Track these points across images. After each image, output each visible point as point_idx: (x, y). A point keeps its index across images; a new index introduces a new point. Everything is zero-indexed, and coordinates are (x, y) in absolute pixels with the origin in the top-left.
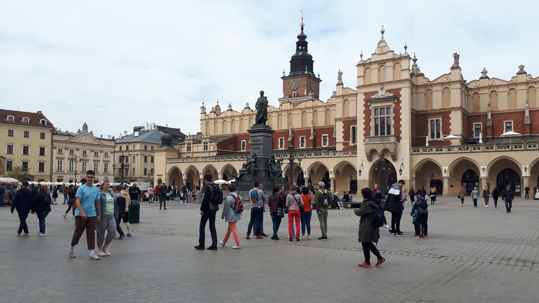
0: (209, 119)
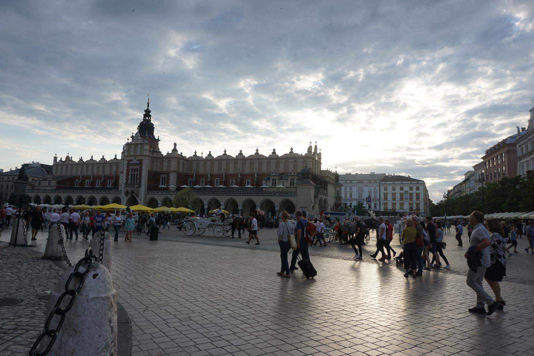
0: (59, 165)
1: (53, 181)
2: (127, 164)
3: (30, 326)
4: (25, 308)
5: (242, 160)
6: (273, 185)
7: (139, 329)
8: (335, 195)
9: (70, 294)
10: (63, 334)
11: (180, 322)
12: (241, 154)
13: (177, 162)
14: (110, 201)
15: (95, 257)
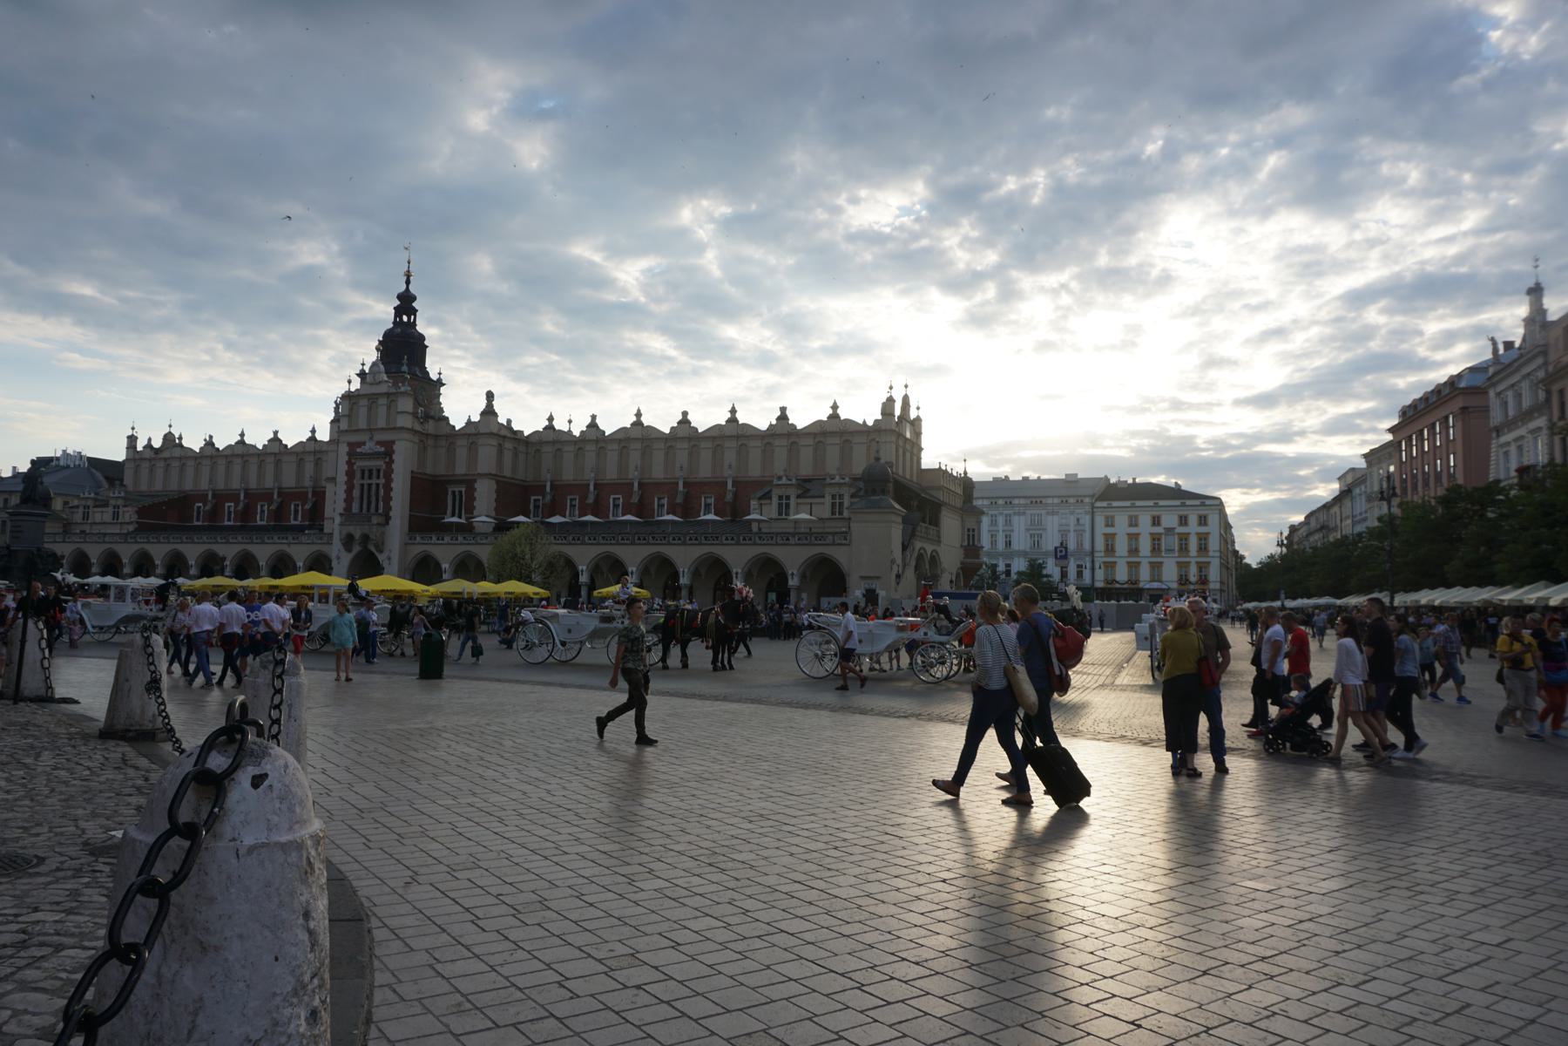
1: (125, 509)
2: (349, 454)
3: (65, 935)
4: (50, 883)
5: (689, 439)
6: (780, 514)
7: (394, 937)
8: (963, 541)
9: (185, 837)
10: (165, 953)
11: (514, 916)
12: (685, 421)
14: (300, 564)
15: (255, 723)
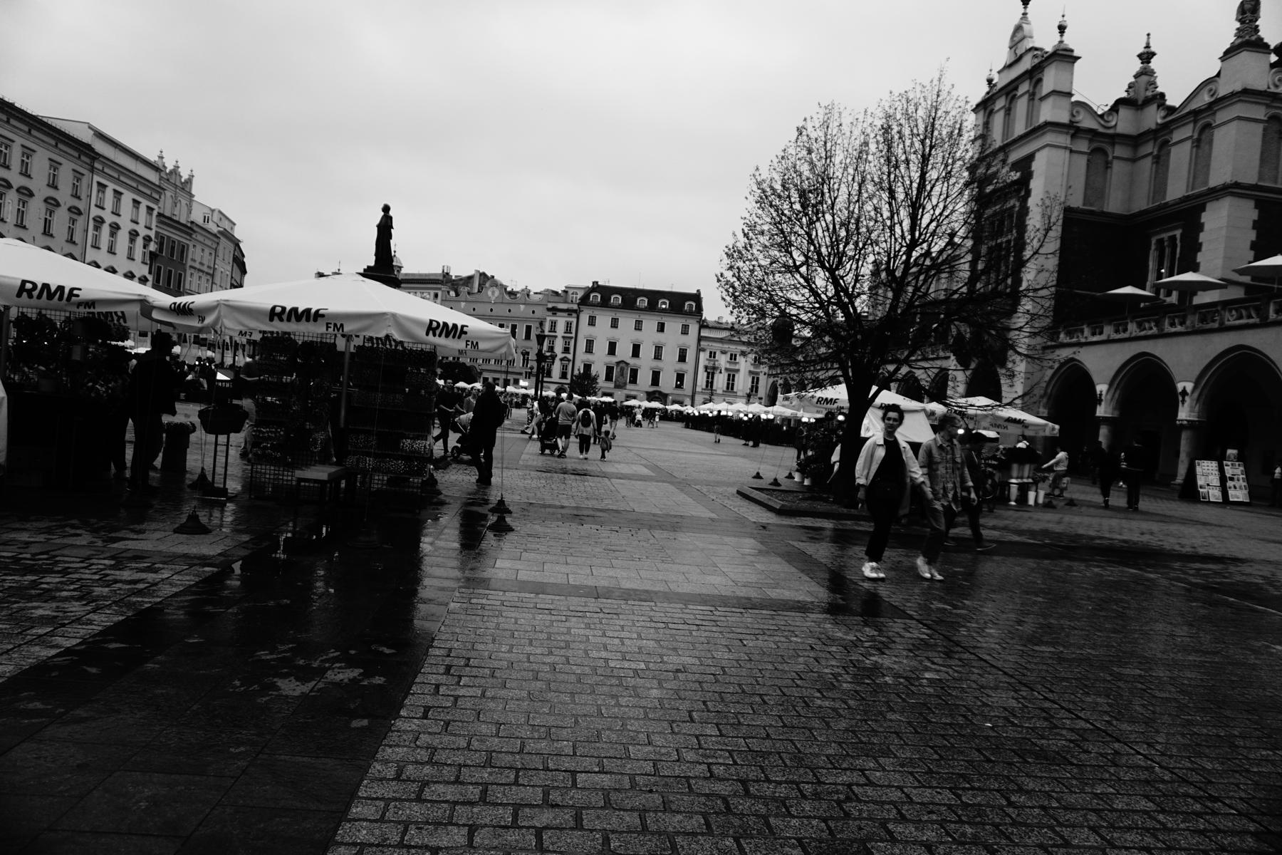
13: (1259, 128)
